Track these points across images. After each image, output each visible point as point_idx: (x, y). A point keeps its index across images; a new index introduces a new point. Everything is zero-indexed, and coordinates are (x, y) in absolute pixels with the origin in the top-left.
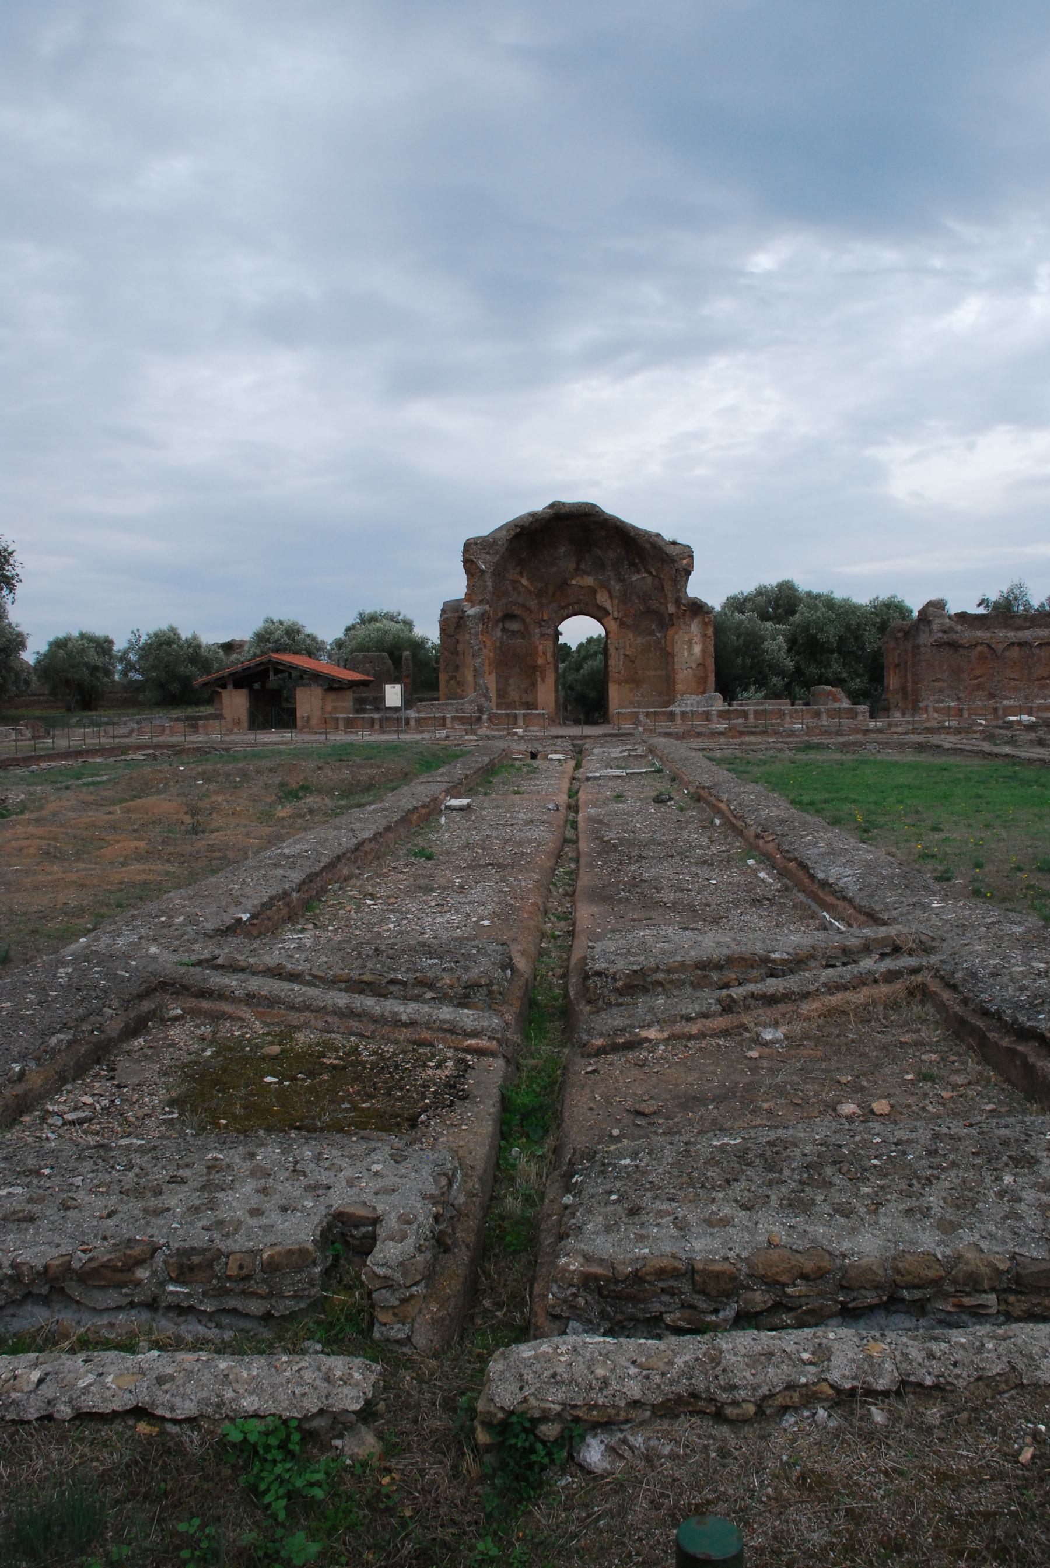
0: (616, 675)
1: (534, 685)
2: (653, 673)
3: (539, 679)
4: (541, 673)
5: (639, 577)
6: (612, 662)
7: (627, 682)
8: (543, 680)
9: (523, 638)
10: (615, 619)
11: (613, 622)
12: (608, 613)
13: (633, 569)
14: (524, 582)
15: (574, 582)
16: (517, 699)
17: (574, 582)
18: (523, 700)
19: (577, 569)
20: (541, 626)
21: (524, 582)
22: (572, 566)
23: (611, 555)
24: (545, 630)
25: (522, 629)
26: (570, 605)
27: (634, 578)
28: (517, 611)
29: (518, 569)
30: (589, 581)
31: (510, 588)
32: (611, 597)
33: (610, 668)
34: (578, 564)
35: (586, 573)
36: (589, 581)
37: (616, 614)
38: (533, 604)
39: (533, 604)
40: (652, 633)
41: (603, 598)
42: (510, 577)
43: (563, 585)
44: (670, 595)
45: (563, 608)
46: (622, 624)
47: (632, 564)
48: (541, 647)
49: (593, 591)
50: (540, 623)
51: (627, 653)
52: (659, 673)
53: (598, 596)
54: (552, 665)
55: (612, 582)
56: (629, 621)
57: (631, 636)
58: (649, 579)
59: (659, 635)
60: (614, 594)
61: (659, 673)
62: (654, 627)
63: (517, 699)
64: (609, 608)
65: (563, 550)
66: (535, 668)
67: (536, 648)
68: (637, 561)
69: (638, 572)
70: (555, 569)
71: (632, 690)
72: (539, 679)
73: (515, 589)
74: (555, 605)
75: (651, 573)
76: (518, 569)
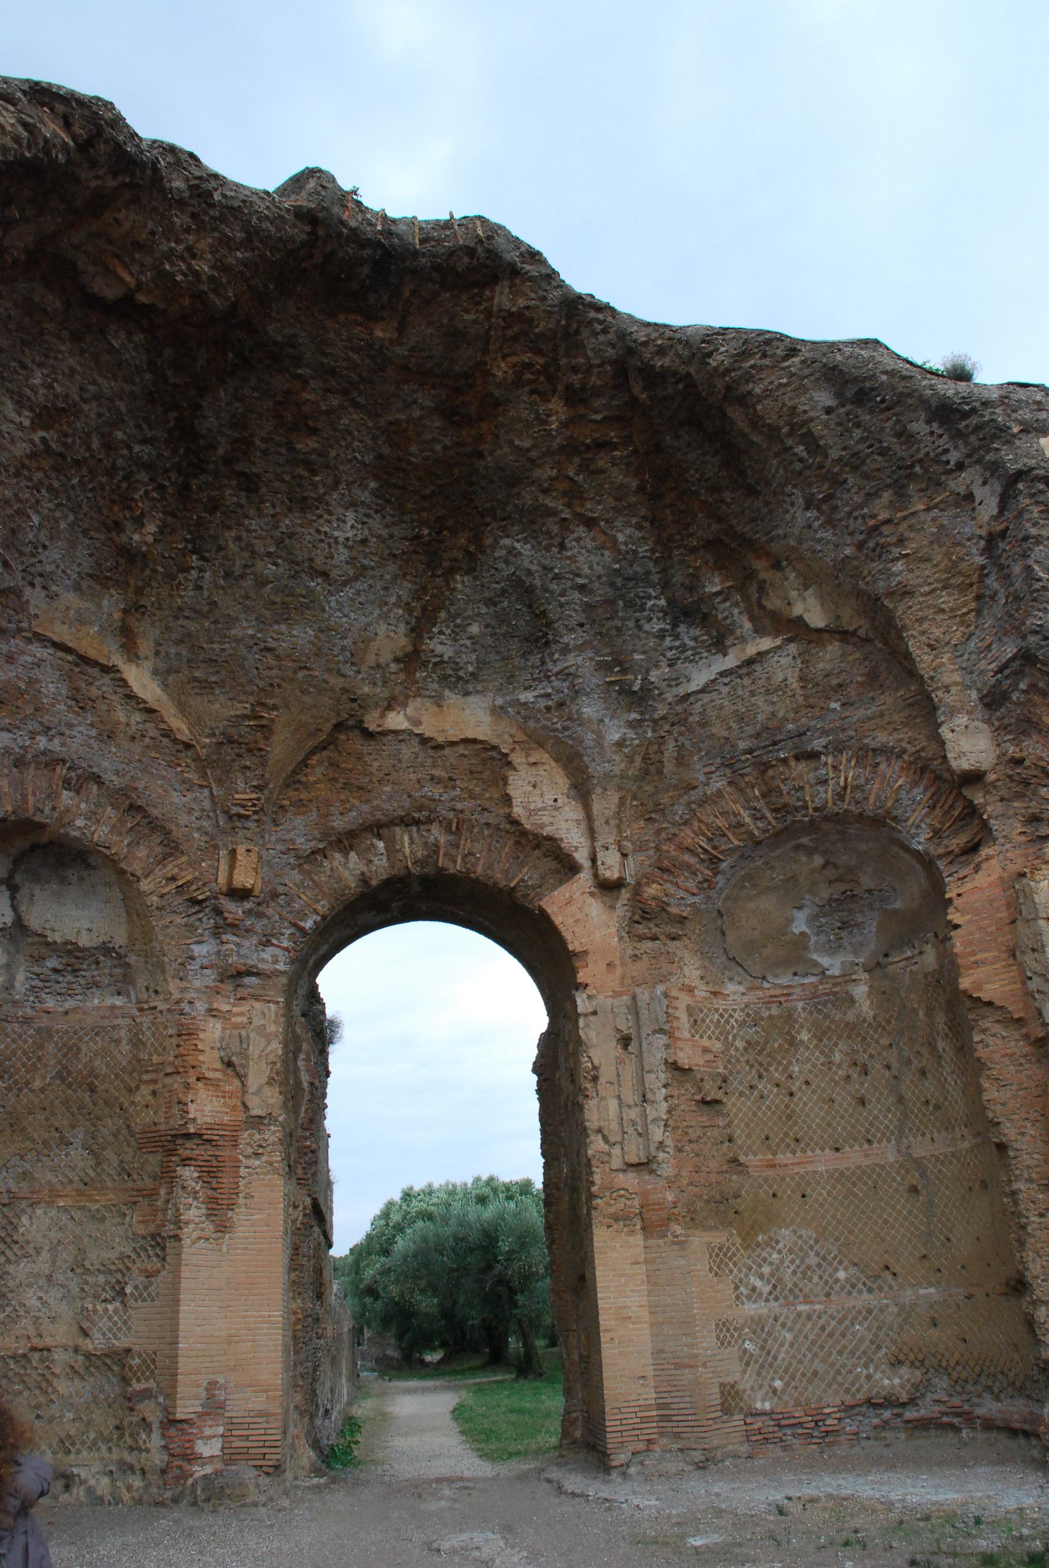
0: (630, 1180)
1: (162, 1243)
2: (823, 1162)
3: (194, 1212)
4: (210, 1173)
5: (730, 662)
6: (602, 1111)
7: (693, 1220)
8: (219, 1210)
9: (123, 984)
10: (608, 888)
11: (595, 909)
12: (568, 868)
13: (688, 634)
14: (141, 680)
15: (396, 720)
16: (60, 1334)
17: (396, 720)
18: (96, 1343)
19: (411, 660)
20: (223, 926)
21: (141, 680)
22: (390, 638)
23: (586, 557)
24: (243, 950)
25: (120, 939)
26: (377, 828)
27: (699, 678)
28: (87, 820)
29: (112, 604)
30: (471, 717)
31: (52, 686)
32: (582, 790)
33: (596, 1145)
34: (417, 632)
35: (458, 680)
36: (471, 717)
37: (611, 866)
38: (180, 802)
39: (180, 802)
40: (794, 955)
41: (540, 796)
42: (61, 633)
43: (350, 727)
44: (951, 676)
45: (346, 841)
46: (647, 918)
47: (689, 611)
48: (212, 1032)
49: (490, 762)
50: (219, 908)
51: (685, 1057)
52: (854, 1157)
53: (518, 786)
54: (273, 1134)
55: (590, 709)
56: (680, 895)
57: (691, 971)
58: (785, 666)
59: (833, 964)
60: (597, 769)
61: (854, 1157)
62: (800, 924)
63: (60, 1334)
64: (573, 837)
65: (346, 528)
66: (173, 1143)
67: (187, 1033)
68: (714, 585)
69: (719, 645)
70: (301, 635)
71: (720, 1259)
72: (194, 1212)
73: (81, 703)
74: (299, 830)
75: (795, 629)
76: (112, 604)
